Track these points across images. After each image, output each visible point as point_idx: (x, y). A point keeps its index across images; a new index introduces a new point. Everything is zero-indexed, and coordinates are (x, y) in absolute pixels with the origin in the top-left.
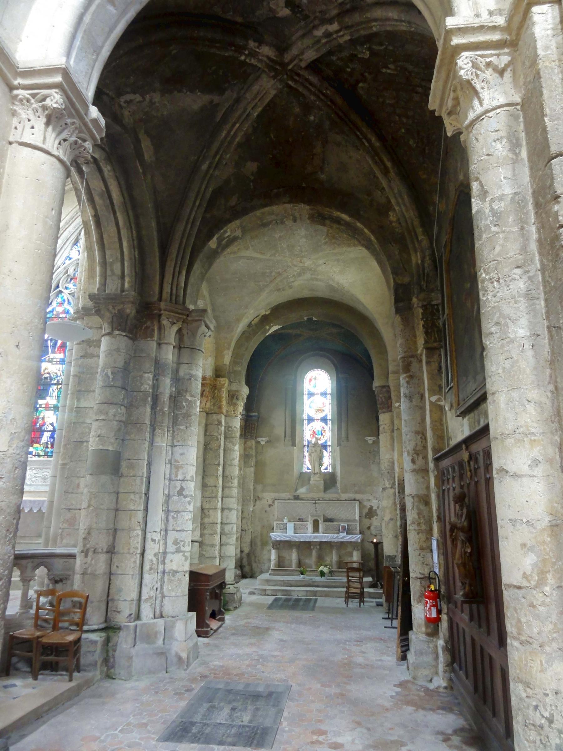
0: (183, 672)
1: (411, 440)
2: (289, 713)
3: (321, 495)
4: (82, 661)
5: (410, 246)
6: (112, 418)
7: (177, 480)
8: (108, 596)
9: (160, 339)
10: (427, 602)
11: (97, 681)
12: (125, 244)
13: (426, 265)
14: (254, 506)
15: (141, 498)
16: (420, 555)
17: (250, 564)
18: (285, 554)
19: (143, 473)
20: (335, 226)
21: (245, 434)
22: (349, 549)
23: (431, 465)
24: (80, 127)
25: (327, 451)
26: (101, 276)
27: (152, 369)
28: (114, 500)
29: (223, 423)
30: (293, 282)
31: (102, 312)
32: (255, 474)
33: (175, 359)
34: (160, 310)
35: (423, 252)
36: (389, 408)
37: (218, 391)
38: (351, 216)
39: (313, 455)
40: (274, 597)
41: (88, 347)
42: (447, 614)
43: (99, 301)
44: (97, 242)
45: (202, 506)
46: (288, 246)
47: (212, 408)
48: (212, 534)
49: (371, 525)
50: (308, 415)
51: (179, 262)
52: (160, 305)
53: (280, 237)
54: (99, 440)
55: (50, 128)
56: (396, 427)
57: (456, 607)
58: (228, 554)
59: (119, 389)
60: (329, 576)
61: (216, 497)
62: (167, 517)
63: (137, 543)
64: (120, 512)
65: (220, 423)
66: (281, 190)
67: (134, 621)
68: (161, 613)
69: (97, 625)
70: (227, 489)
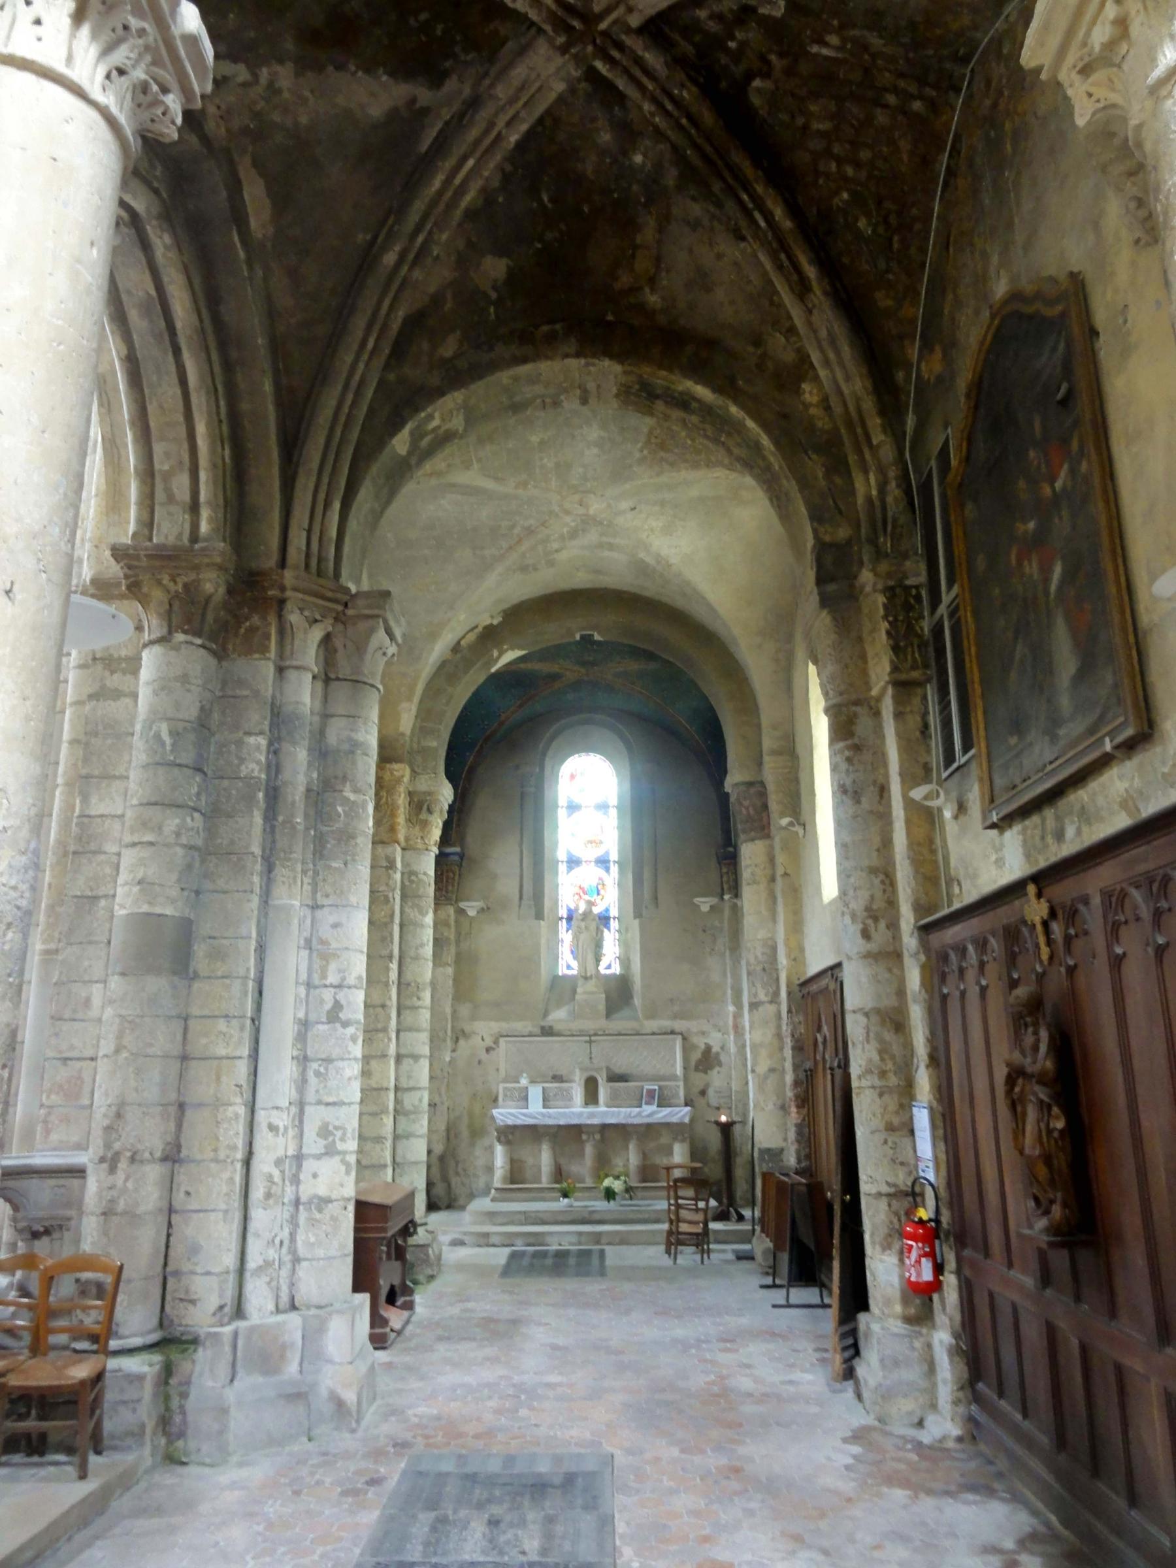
0: (347, 1435)
1: (860, 888)
2: (628, 1524)
3: (602, 1023)
4: (108, 1426)
5: (852, 459)
6: (171, 839)
7: (326, 986)
8: (165, 1264)
9: (281, 655)
10: (911, 1246)
11: (147, 1472)
12: (201, 429)
13: (890, 499)
14: (454, 1051)
15: (242, 1028)
16: (886, 1142)
17: (445, 1179)
18: (525, 1154)
19: (248, 970)
20: (677, 414)
22: (664, 1140)
23: (910, 941)
24: (157, 49)
26: (140, 504)
27: (266, 726)
28: (179, 1037)
29: (399, 865)
30: (557, 551)
31: (145, 589)
32: (456, 980)
33: (318, 705)
34: (283, 589)
35: (882, 471)
36: (763, 829)
37: (388, 792)
38: (717, 389)
39: (582, 937)
40: (507, 1251)
41: (107, 673)
42: (958, 1272)
43: (136, 563)
44: (133, 424)
46: (558, 465)
49: (707, 1085)
50: (569, 853)
51: (325, 480)
52: (282, 577)
53: (542, 443)
54: (141, 890)
55: (85, 31)
56: (780, 871)
57: (987, 1254)
58: (411, 1157)
59: (189, 772)
60: (625, 1199)
61: (385, 1030)
62: (304, 1072)
63: (235, 1134)
64: (193, 1064)
66: (558, 327)
67: (229, 1323)
68: (293, 1299)
69: (142, 1335)
70: (408, 1012)
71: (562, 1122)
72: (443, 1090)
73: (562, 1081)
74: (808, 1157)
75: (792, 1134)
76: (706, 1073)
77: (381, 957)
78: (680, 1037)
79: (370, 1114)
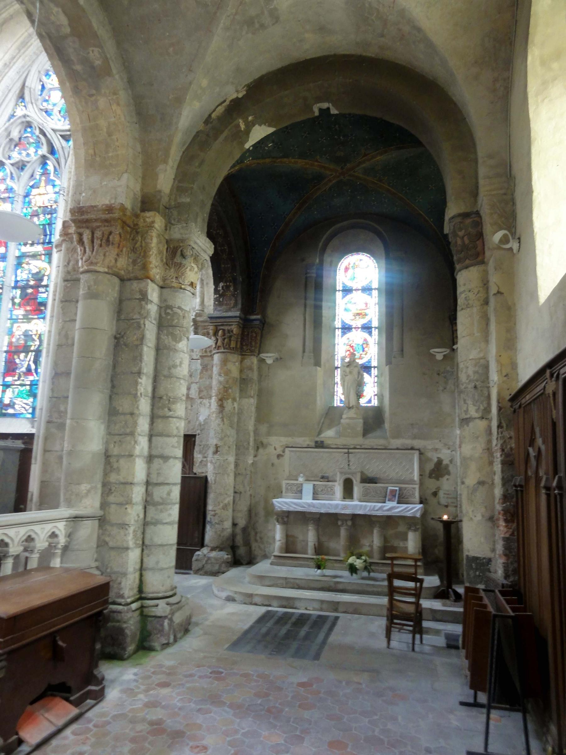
3: (359, 440)
14: (255, 456)
17: (247, 543)
18: (297, 531)
21: (242, 348)
22: (402, 528)
25: (370, 375)
32: (258, 409)
37: (142, 237)
39: (347, 378)
40: (264, 609)
45: (107, 450)
47: (130, 268)
48: (121, 504)
49: (439, 489)
50: (343, 322)
56: (493, 290)
58: (158, 540)
65: (144, 297)
70: (160, 420)
71: (323, 511)
73: (328, 481)
74: (516, 572)
75: (500, 547)
76: (438, 480)
77: (132, 373)
78: (417, 452)
79: (117, 504)
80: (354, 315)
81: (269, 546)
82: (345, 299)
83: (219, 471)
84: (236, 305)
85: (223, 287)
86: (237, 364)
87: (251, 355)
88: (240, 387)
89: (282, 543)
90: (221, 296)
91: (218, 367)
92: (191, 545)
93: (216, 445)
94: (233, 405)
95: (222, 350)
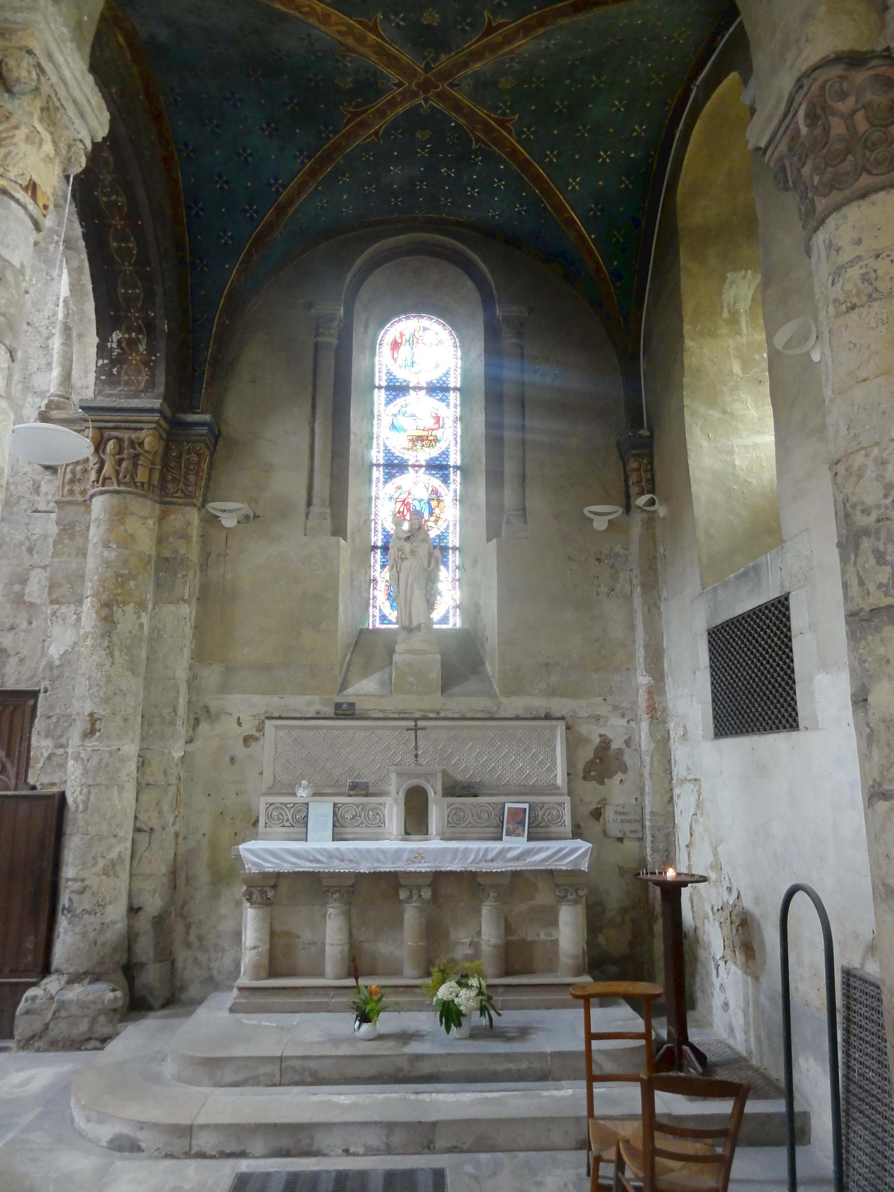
3: (434, 701)
14: (190, 741)
17: (166, 956)
22: (544, 898)
32: (199, 629)
39: (405, 565)
49: (604, 802)
50: (387, 452)
71: (364, 868)
72: (166, 807)
73: (366, 795)
76: (602, 783)
80: (412, 440)
81: (219, 955)
82: (391, 405)
83: (98, 780)
84: (151, 384)
85: (119, 342)
86: (150, 522)
87: (186, 505)
88: (157, 577)
89: (259, 954)
90: (114, 362)
91: (103, 528)
92: (14, 973)
93: (91, 715)
94: (139, 617)
95: (115, 487)
